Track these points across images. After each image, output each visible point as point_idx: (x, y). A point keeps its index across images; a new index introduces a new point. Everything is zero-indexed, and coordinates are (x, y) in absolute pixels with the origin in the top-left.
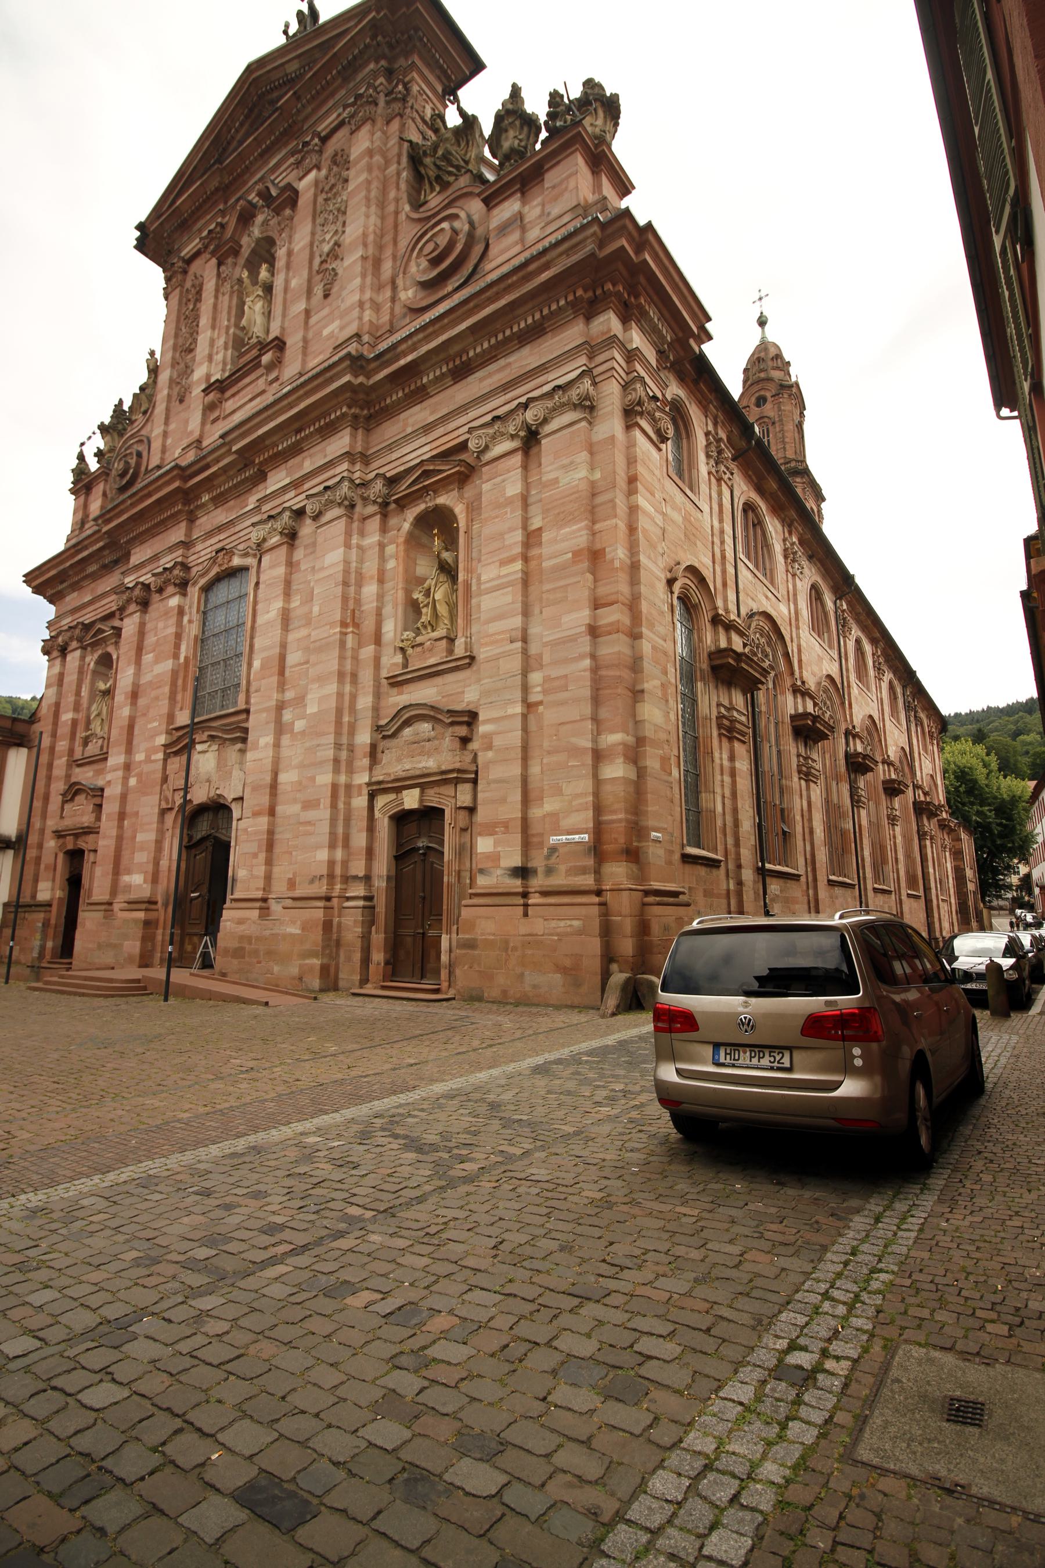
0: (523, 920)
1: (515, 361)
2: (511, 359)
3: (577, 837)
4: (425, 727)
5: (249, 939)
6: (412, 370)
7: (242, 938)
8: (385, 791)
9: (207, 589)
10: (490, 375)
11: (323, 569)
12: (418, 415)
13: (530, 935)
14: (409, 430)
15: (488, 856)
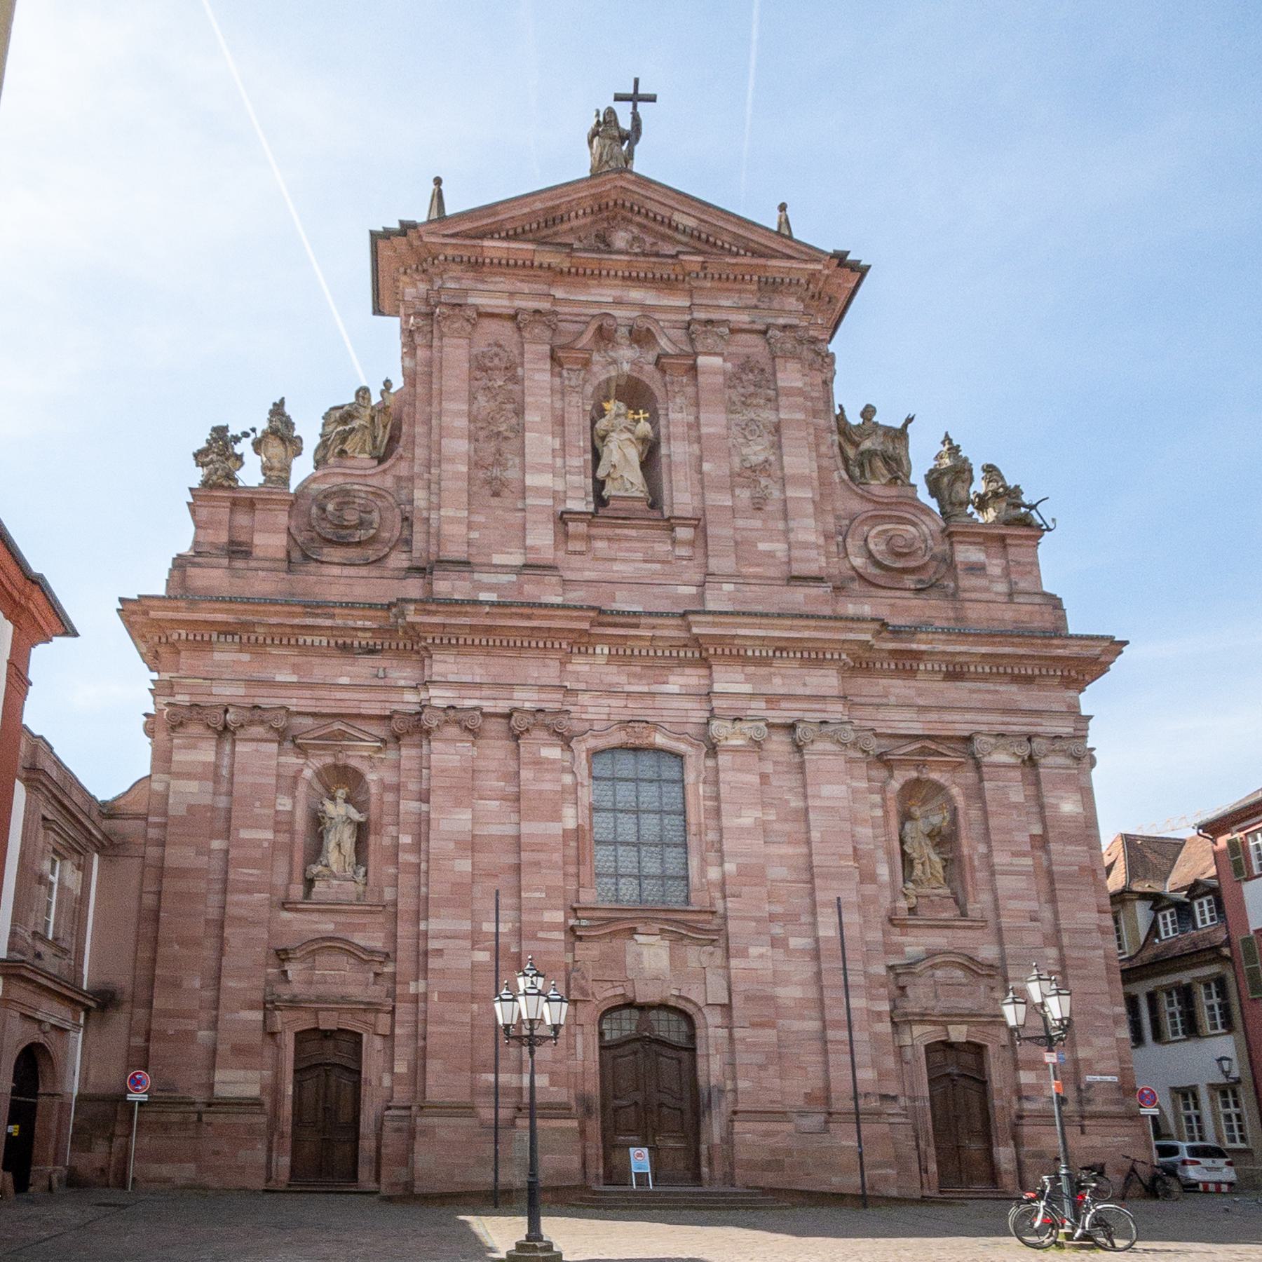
0: (1083, 1137)
1: (1006, 692)
2: (1002, 688)
3: (1109, 1078)
4: (959, 973)
5: (789, 1152)
6: (917, 655)
7: (773, 1151)
8: (922, 1022)
9: (595, 754)
10: (979, 691)
11: (819, 797)
12: (899, 688)
13: (1092, 1147)
14: (893, 700)
15: (1032, 1087)
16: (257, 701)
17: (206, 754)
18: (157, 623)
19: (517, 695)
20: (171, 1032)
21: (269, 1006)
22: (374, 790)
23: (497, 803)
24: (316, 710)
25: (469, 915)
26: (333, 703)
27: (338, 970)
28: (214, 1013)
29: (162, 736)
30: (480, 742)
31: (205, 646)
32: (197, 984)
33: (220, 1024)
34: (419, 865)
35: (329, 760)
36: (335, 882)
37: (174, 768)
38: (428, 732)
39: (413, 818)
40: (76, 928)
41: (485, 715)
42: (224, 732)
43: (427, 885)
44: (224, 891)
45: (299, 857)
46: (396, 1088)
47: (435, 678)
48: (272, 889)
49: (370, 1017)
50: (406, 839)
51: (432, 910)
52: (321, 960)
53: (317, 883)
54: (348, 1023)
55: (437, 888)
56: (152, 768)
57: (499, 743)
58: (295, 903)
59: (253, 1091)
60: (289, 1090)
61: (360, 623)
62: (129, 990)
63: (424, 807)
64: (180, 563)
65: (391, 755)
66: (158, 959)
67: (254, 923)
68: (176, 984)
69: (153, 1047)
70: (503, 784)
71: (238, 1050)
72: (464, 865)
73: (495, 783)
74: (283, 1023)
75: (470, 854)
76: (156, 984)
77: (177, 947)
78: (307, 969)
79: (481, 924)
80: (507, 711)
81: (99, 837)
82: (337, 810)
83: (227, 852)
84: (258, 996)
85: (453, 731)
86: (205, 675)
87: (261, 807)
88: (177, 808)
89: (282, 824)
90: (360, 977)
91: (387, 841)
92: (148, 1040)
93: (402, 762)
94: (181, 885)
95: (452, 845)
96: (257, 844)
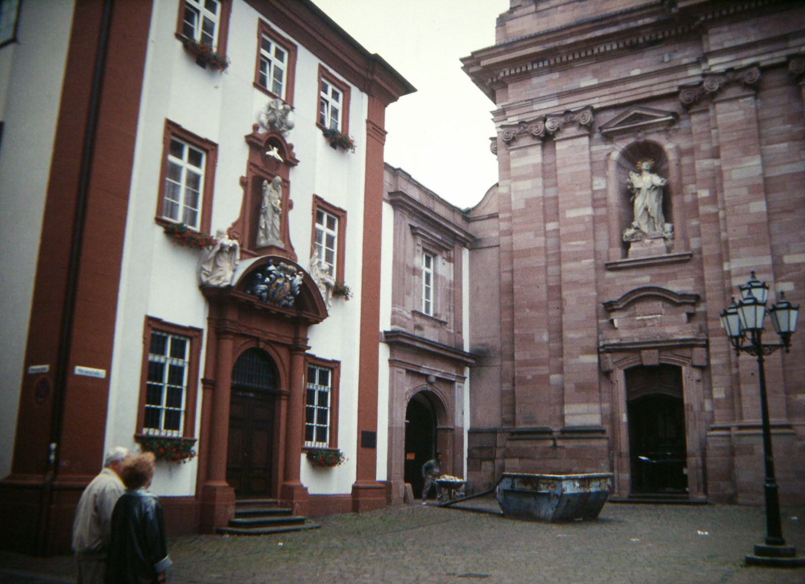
16: (568, 107)
17: (535, 156)
18: (488, 68)
19: (792, 43)
20: (529, 377)
21: (602, 351)
22: (672, 156)
23: (786, 145)
24: (616, 102)
25: (768, 251)
26: (628, 94)
27: (655, 314)
28: (560, 359)
29: (502, 151)
30: (763, 94)
31: (525, 76)
32: (545, 338)
33: (565, 368)
34: (717, 214)
35: (631, 140)
36: (647, 241)
37: (513, 173)
38: (713, 95)
39: (709, 174)
40: (452, 304)
41: (765, 70)
42: (547, 139)
43: (726, 230)
44: (559, 262)
45: (615, 224)
46: (716, 412)
47: (713, 49)
48: (596, 254)
49: (686, 352)
50: (704, 193)
51: (732, 252)
52: (640, 307)
53: (632, 245)
54: (670, 358)
55: (735, 231)
56: (499, 178)
57: (780, 90)
58: (616, 263)
59: (594, 420)
60: (624, 418)
61: (640, 22)
62: (498, 345)
63: (716, 162)
64: (502, 21)
65: (684, 124)
66: (515, 322)
67: (586, 284)
68: (529, 340)
69: (517, 389)
70: (789, 126)
71: (580, 387)
72: (759, 206)
73: (782, 127)
74: (614, 363)
75: (763, 194)
76: (516, 342)
77: (528, 310)
78: (630, 316)
79: (781, 257)
80: (783, 59)
81: (463, 235)
82: (645, 180)
83: (558, 230)
84: (592, 343)
85: (732, 92)
86: (527, 98)
87: (581, 189)
88: (518, 203)
89: (597, 201)
90: (674, 318)
91: (688, 199)
92: (514, 385)
93: (694, 128)
94: (526, 262)
95: (744, 192)
96: (579, 220)
